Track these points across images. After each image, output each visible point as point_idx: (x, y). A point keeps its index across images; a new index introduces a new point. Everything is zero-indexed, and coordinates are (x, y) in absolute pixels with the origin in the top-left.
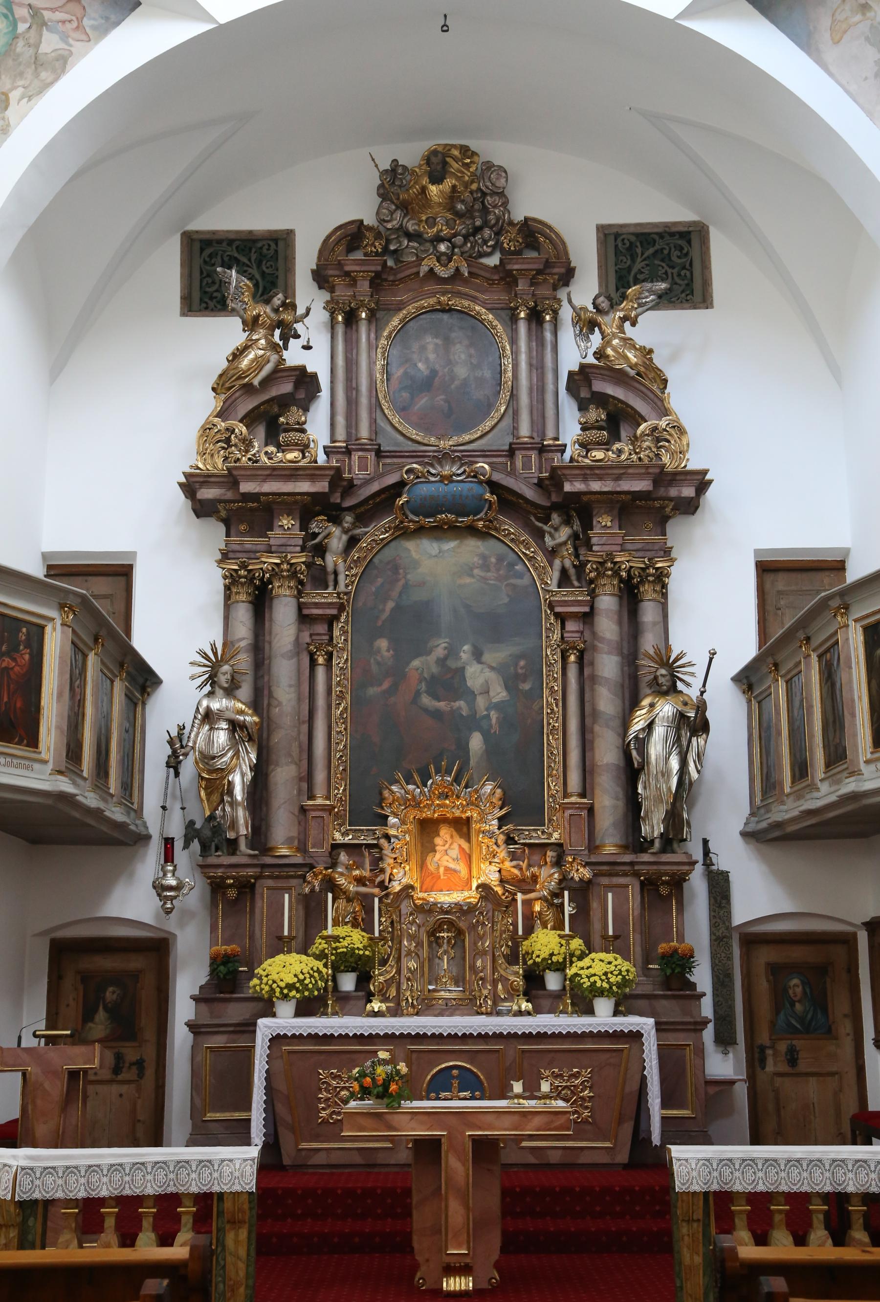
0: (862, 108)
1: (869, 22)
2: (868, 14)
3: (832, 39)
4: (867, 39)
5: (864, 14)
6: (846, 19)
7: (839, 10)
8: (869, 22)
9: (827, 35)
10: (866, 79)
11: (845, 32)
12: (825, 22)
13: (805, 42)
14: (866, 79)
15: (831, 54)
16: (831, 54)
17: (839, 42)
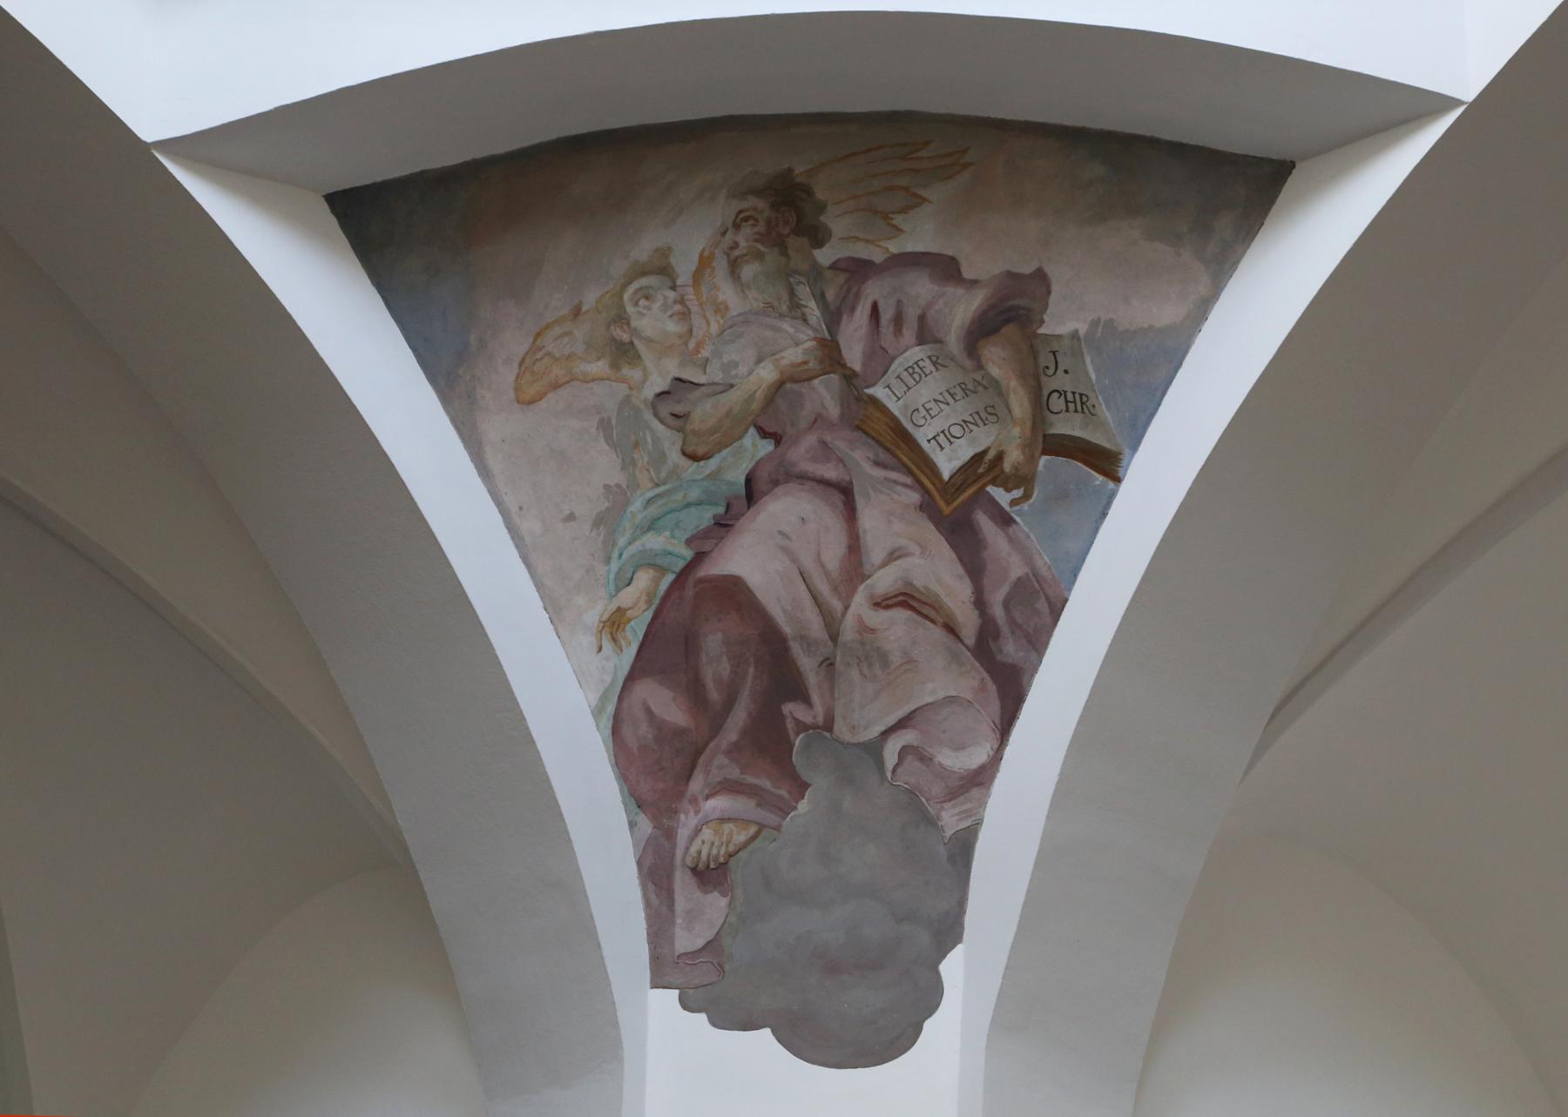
0: (539, 586)
1: (622, 390)
2: (626, 371)
3: (517, 389)
4: (604, 425)
5: (615, 366)
6: (569, 357)
7: (557, 330)
8: (622, 390)
9: (506, 376)
10: (571, 517)
11: (555, 386)
12: (514, 343)
13: (447, 366)
14: (571, 517)
15: (499, 425)
16: (499, 425)
17: (531, 402)
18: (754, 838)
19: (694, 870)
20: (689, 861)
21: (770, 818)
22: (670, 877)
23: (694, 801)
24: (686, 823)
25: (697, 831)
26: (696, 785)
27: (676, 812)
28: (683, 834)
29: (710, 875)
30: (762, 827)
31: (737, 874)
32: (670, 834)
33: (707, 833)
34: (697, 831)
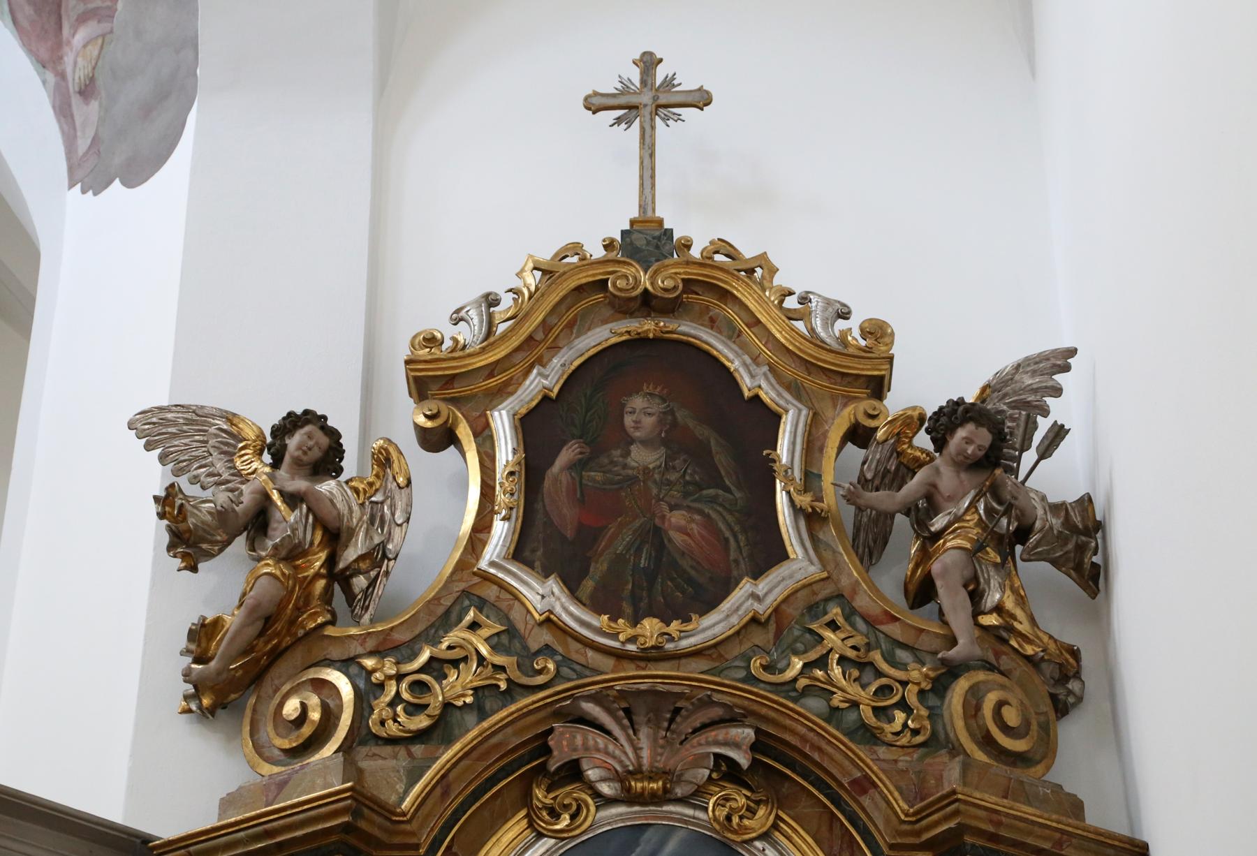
18: (102, 47)
19: (81, 93)
20: (77, 89)
21: (105, 26)
22: (70, 106)
23: (69, 43)
24: (69, 59)
25: (75, 63)
26: (66, 31)
27: (61, 58)
28: (69, 70)
29: (87, 91)
30: (103, 36)
31: (100, 82)
32: (62, 76)
33: (80, 60)
34: (75, 63)
